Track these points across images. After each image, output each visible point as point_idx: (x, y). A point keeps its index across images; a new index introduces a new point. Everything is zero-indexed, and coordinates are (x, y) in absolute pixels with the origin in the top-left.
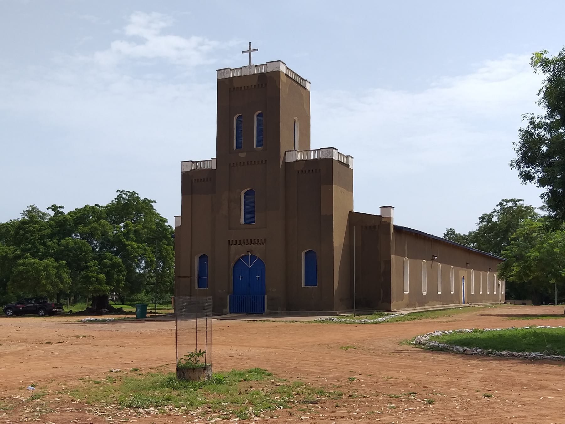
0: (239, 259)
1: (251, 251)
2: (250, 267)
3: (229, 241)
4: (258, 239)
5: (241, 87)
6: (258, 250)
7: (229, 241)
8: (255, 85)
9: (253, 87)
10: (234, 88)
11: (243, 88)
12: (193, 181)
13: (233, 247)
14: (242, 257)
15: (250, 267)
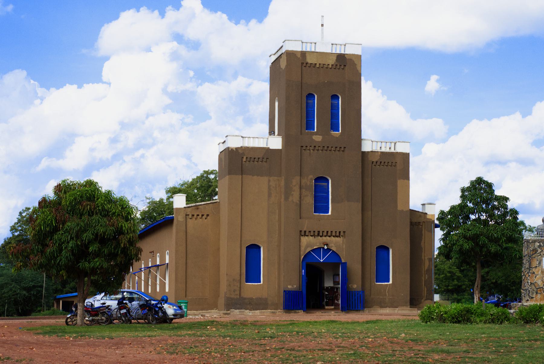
0: (309, 252)
1: (327, 245)
2: (322, 261)
3: (301, 231)
4: (332, 232)
5: (316, 64)
6: (335, 243)
7: (301, 231)
8: (332, 65)
9: (330, 66)
10: (307, 63)
11: (318, 66)
12: (244, 159)
13: (305, 240)
14: (313, 250)
15: (322, 261)
